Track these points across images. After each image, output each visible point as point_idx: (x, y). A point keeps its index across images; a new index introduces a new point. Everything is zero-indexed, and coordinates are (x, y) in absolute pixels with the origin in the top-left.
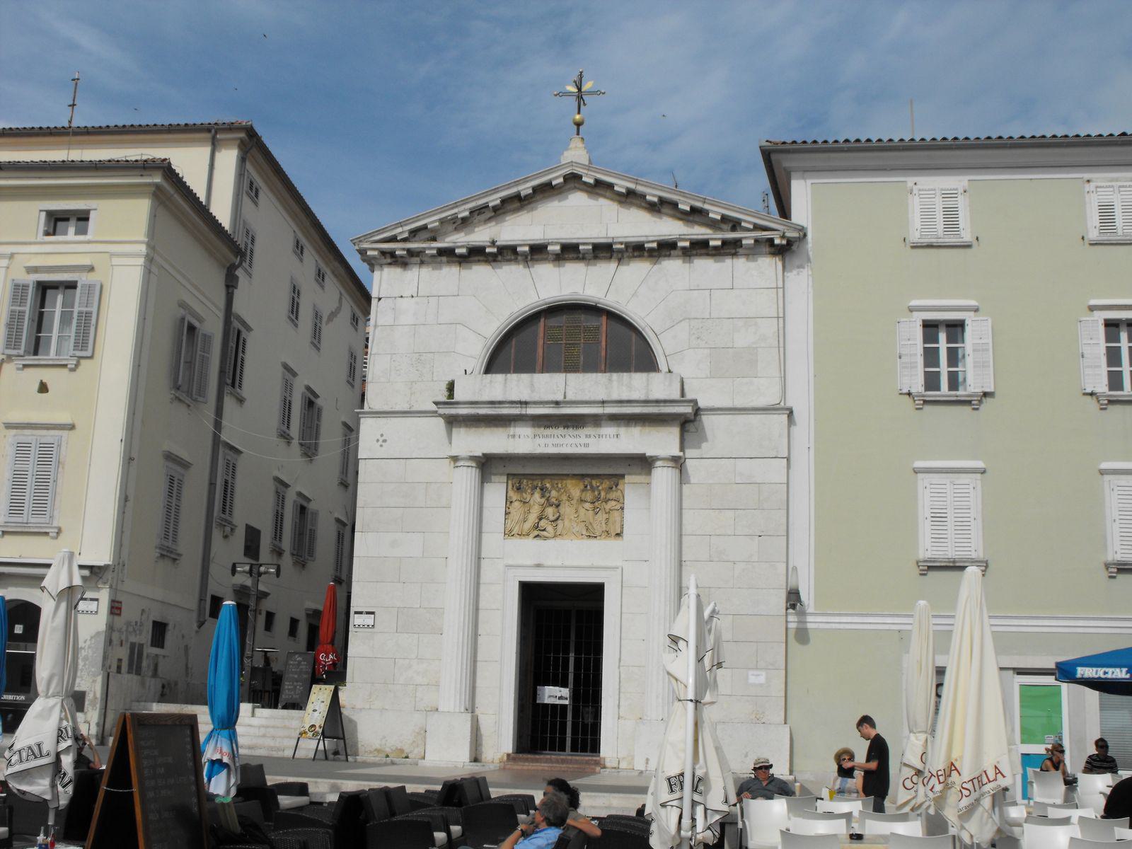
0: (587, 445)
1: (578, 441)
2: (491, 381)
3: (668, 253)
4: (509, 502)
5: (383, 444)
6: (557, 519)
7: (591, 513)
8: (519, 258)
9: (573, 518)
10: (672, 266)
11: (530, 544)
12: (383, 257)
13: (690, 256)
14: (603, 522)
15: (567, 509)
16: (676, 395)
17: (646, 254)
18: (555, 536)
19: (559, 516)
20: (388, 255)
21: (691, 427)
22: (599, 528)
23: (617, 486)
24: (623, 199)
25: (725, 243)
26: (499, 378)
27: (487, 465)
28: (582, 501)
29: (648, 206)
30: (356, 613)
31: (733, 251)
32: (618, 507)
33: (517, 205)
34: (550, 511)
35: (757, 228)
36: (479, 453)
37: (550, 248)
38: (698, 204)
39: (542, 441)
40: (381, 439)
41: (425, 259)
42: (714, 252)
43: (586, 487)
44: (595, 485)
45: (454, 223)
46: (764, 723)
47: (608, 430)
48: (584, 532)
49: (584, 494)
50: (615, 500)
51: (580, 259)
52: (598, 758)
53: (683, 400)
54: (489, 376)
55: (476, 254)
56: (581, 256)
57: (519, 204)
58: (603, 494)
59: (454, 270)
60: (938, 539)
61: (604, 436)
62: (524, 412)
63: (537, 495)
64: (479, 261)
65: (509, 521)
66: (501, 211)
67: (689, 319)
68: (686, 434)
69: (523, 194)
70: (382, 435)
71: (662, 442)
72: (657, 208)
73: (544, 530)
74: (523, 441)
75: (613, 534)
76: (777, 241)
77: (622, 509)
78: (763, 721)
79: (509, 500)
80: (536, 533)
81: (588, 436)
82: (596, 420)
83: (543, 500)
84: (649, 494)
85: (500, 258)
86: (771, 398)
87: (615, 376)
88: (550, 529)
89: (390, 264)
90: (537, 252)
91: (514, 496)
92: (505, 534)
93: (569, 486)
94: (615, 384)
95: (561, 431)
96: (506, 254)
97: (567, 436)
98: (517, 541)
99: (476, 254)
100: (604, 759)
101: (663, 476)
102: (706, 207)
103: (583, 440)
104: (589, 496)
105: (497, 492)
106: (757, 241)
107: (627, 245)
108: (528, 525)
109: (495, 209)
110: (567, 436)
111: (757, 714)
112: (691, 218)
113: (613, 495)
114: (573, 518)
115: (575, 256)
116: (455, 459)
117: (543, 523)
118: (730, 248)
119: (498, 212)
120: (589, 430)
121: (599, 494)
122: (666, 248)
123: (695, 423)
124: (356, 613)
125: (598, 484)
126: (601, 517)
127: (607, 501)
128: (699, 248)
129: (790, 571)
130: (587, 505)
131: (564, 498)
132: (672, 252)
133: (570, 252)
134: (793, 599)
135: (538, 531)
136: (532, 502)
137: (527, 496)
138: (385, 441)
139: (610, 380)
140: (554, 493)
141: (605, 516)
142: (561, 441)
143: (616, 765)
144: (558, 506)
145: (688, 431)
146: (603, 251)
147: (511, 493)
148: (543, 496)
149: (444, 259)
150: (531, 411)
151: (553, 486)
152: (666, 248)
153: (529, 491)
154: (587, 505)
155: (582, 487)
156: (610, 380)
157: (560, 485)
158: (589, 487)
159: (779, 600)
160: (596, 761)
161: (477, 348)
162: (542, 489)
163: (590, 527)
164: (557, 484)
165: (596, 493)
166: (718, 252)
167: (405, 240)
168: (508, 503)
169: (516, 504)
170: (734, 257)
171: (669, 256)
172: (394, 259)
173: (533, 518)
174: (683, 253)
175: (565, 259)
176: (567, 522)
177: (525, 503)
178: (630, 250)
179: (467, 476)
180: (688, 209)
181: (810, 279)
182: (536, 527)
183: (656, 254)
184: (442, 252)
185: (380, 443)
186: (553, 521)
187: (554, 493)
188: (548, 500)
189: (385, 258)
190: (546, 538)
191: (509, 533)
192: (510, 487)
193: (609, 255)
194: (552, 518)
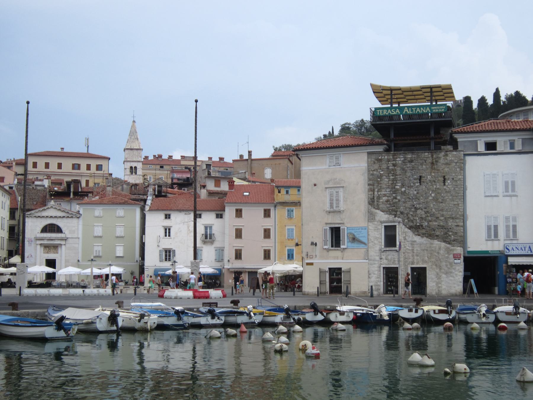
10: (64, 219)
15: (51, 250)
16: (65, 237)
26: (42, 234)
27: (41, 244)
35: (75, 215)
53: (66, 237)
55: (39, 217)
59: (36, 218)
60: (96, 253)
71: (63, 242)
74: (46, 242)
82: (55, 239)
84: (61, 248)
86: (76, 236)
90: (47, 217)
96: (43, 217)
98: (45, 254)
99: (39, 217)
101: (63, 247)
105: (42, 248)
116: (37, 244)
118: (72, 217)
122: (64, 217)
128: (68, 217)
129: (78, 257)
133: (51, 217)
134: (79, 261)
135: (48, 253)
146: (56, 217)
152: (64, 217)
159: (76, 261)
161: (39, 229)
173: (47, 251)
179: (39, 247)
191: (44, 253)
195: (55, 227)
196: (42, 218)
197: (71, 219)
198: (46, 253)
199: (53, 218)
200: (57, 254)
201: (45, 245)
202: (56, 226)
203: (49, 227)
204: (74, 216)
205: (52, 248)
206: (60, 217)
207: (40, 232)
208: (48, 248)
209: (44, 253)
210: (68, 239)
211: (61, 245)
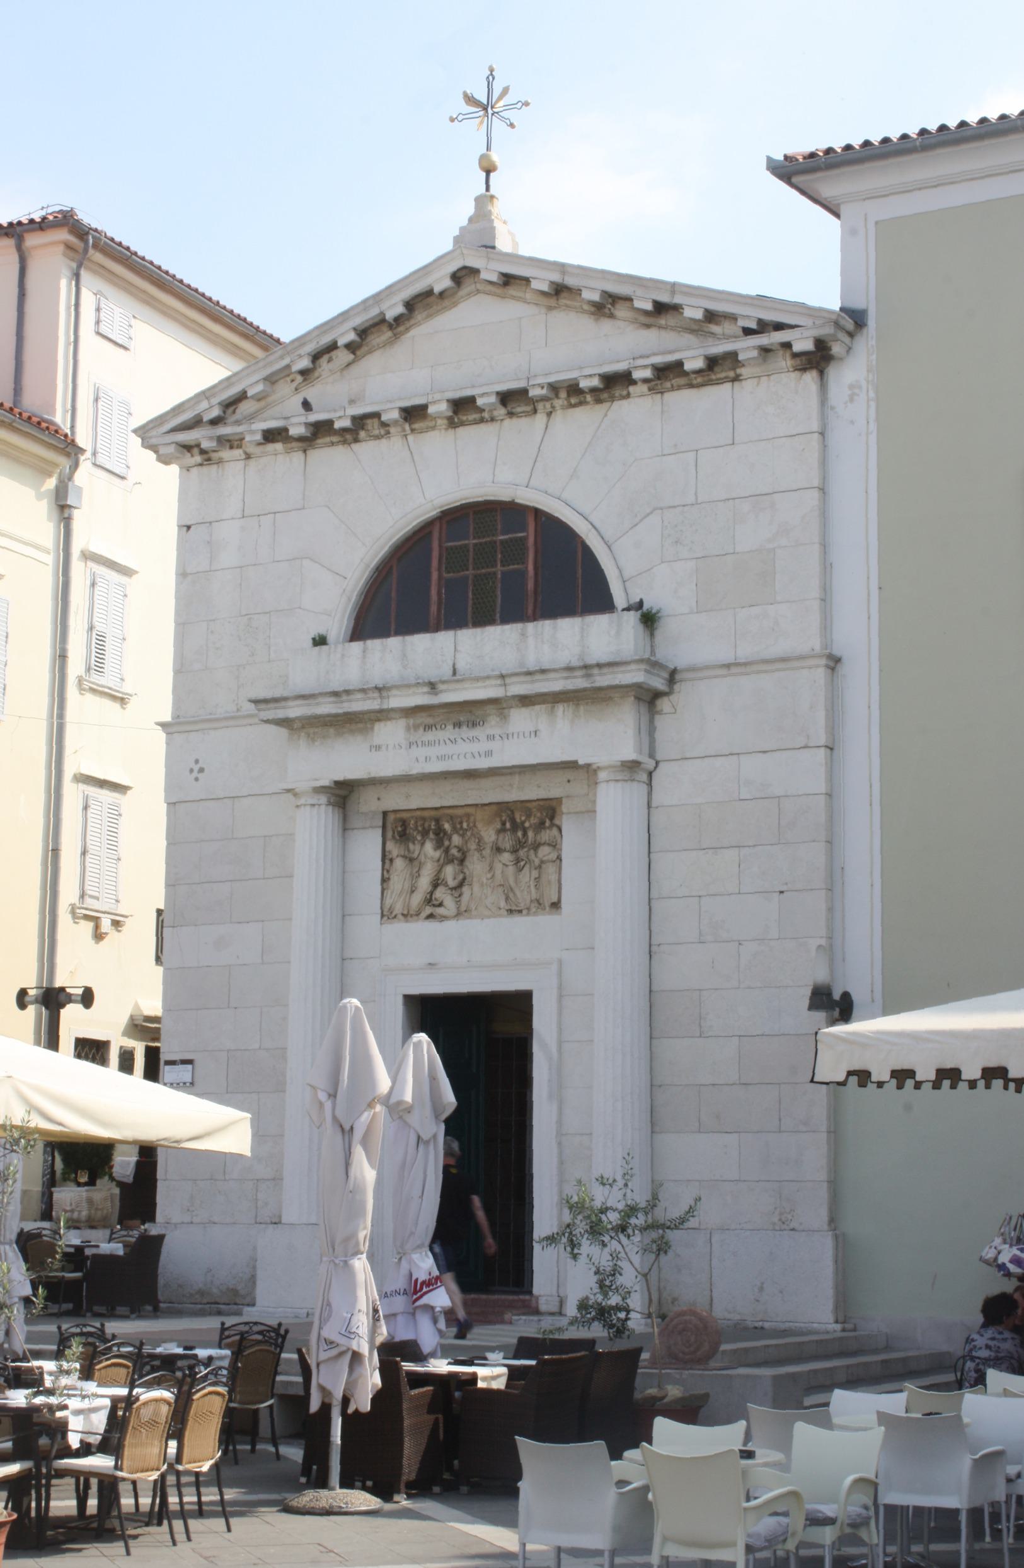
0: (489, 754)
1: (475, 747)
2: (343, 656)
3: (625, 393)
4: (386, 858)
5: (200, 776)
6: (461, 885)
7: (511, 870)
8: (392, 430)
9: (485, 881)
11: (421, 928)
12: (189, 455)
13: (662, 393)
14: (532, 884)
15: (476, 866)
17: (589, 398)
18: (458, 915)
19: (464, 879)
20: (196, 451)
21: (664, 704)
22: (524, 894)
23: (552, 818)
24: (552, 302)
25: (712, 362)
28: (499, 850)
29: (593, 309)
30: (168, 1063)
31: (731, 374)
32: (554, 856)
33: (384, 335)
34: (449, 871)
36: (326, 782)
37: (431, 410)
38: (664, 298)
39: (420, 752)
40: (196, 768)
41: (251, 449)
42: (699, 380)
43: (504, 824)
44: (518, 820)
45: (292, 381)
46: (793, 1230)
47: (521, 719)
48: (503, 904)
49: (501, 836)
50: (549, 845)
51: (487, 421)
52: (527, 1297)
54: (357, 646)
55: (321, 430)
56: (486, 415)
57: (390, 334)
58: (530, 834)
59: (298, 457)
61: (515, 736)
62: (385, 706)
63: (429, 847)
64: (333, 444)
65: (389, 892)
66: (364, 349)
67: (661, 509)
68: (657, 717)
69: (390, 315)
70: (197, 762)
72: (607, 311)
73: (440, 905)
75: (547, 905)
76: (797, 347)
77: (559, 858)
78: (792, 1225)
79: (389, 856)
80: (428, 910)
81: (491, 738)
83: (437, 854)
85: (362, 434)
87: (530, 627)
88: (449, 902)
89: (201, 465)
90: (414, 414)
91: (393, 848)
92: (382, 916)
93: (479, 825)
94: (531, 641)
95: (449, 732)
97: (459, 741)
98: (399, 928)
100: (537, 1298)
102: (677, 300)
103: (484, 746)
104: (507, 841)
106: (765, 351)
107: (554, 388)
108: (417, 898)
109: (351, 347)
110: (459, 741)
111: (781, 1214)
112: (662, 322)
113: (545, 836)
114: (485, 881)
115: (476, 416)
117: (440, 893)
119: (358, 353)
120: (493, 726)
121: (525, 834)
123: (671, 697)
124: (168, 1063)
125: (523, 818)
126: (527, 876)
127: (536, 846)
129: (831, 950)
130: (506, 857)
131: (472, 846)
132: (631, 389)
135: (431, 911)
136: (422, 858)
137: (415, 848)
138: (201, 770)
139: (523, 635)
140: (456, 840)
141: (535, 874)
142: (450, 749)
143: (555, 1309)
144: (462, 861)
145: (660, 713)
147: (390, 845)
148: (437, 848)
149: (279, 446)
150: (397, 701)
151: (454, 829)
153: (419, 838)
154: (506, 857)
155: (499, 826)
156: (523, 635)
157: (465, 825)
158: (508, 825)
160: (524, 1301)
162: (437, 834)
163: (511, 895)
164: (461, 823)
165: (520, 834)
166: (706, 378)
167: (214, 422)
168: (387, 862)
169: (399, 863)
170: (736, 384)
171: (628, 396)
172: (205, 456)
173: (424, 883)
174: (650, 389)
175: (462, 424)
176: (476, 888)
177: (411, 860)
178: (563, 394)
180: (649, 306)
181: (873, 404)
182: (429, 900)
183: (605, 395)
184: (271, 436)
185: (195, 774)
186: (455, 888)
187: (456, 840)
188: (447, 851)
189: (192, 456)
190: (444, 918)
191: (387, 915)
192: (389, 834)
193: (529, 408)
194: (452, 883)
195: (516, 551)
196: (367, 449)
197: (717, 395)
198: (406, 916)
199: (483, 418)
200: (546, 921)
201: (395, 800)
202: (530, 534)
203: (454, 559)
204: (747, 347)
205: (489, 835)
206: (572, 393)
207: (337, 624)
208: (440, 838)
209: (387, 915)
210: (684, 694)
211: (589, 771)
